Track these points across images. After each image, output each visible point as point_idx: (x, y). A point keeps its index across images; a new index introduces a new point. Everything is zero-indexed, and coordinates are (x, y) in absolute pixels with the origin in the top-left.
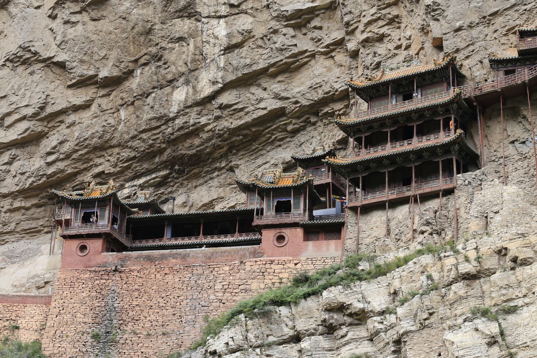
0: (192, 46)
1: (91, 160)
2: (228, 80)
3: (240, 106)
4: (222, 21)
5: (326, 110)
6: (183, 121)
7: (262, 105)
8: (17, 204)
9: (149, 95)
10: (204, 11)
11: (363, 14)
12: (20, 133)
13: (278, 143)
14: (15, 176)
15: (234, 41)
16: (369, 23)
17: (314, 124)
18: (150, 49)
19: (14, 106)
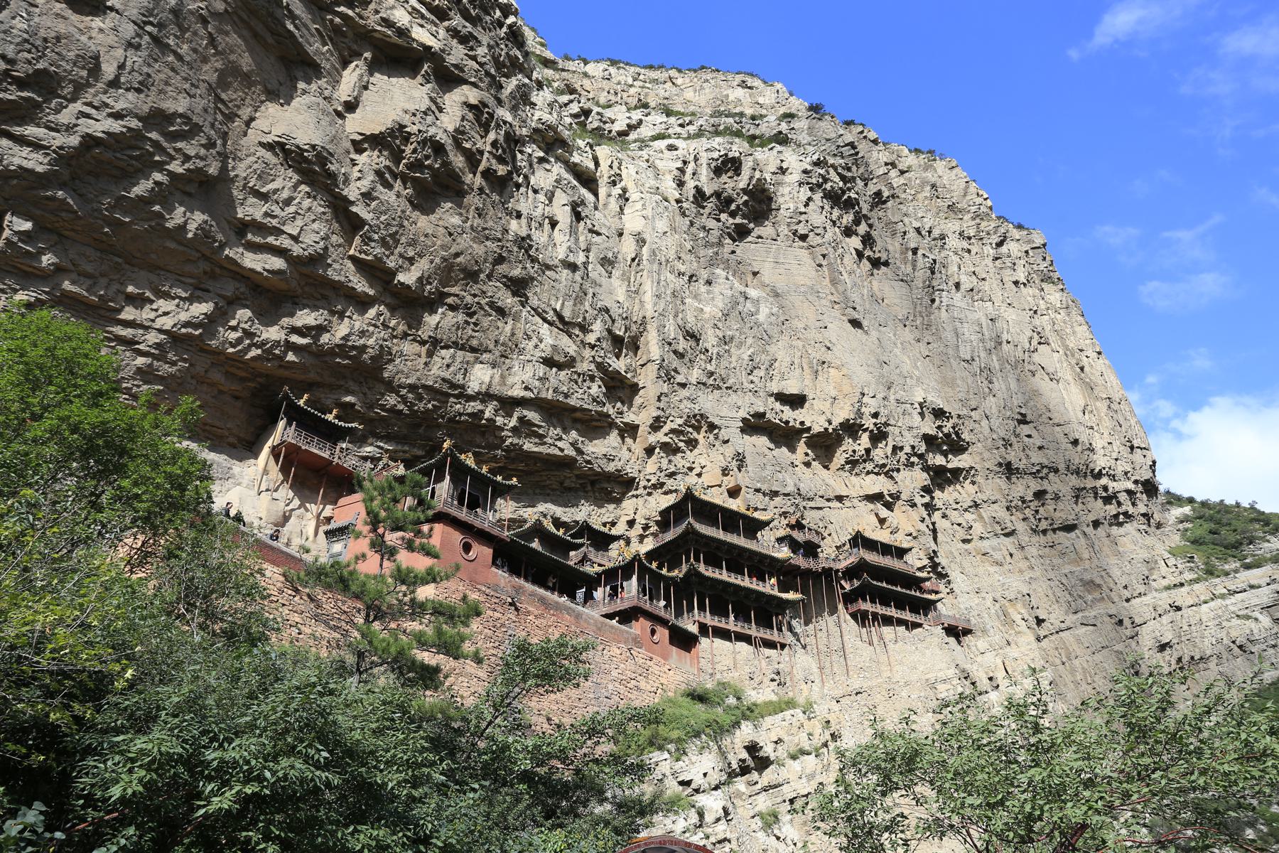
0: (508, 328)
1: (344, 377)
2: (543, 395)
3: (541, 431)
4: (546, 325)
5: (606, 485)
6: (480, 407)
7: (559, 444)
8: (216, 376)
9: (447, 347)
10: (534, 301)
11: (671, 418)
12: (267, 267)
13: (548, 491)
14: (234, 329)
15: (556, 358)
16: (673, 431)
17: (587, 492)
18: (463, 293)
19: (274, 222)
